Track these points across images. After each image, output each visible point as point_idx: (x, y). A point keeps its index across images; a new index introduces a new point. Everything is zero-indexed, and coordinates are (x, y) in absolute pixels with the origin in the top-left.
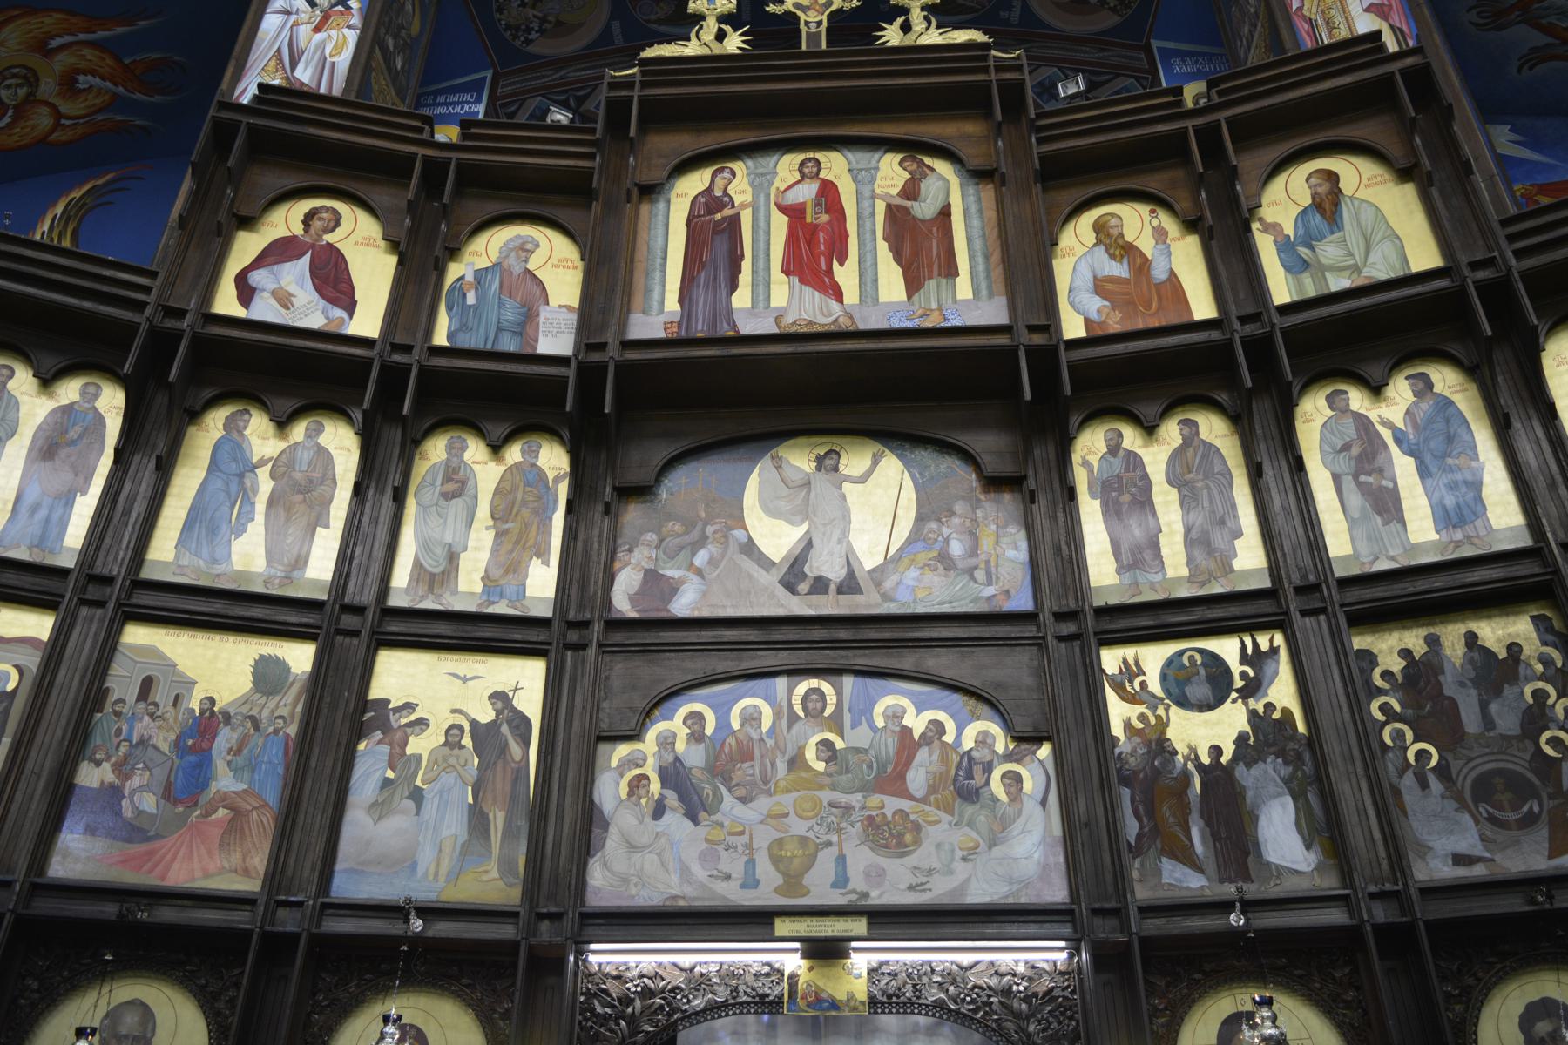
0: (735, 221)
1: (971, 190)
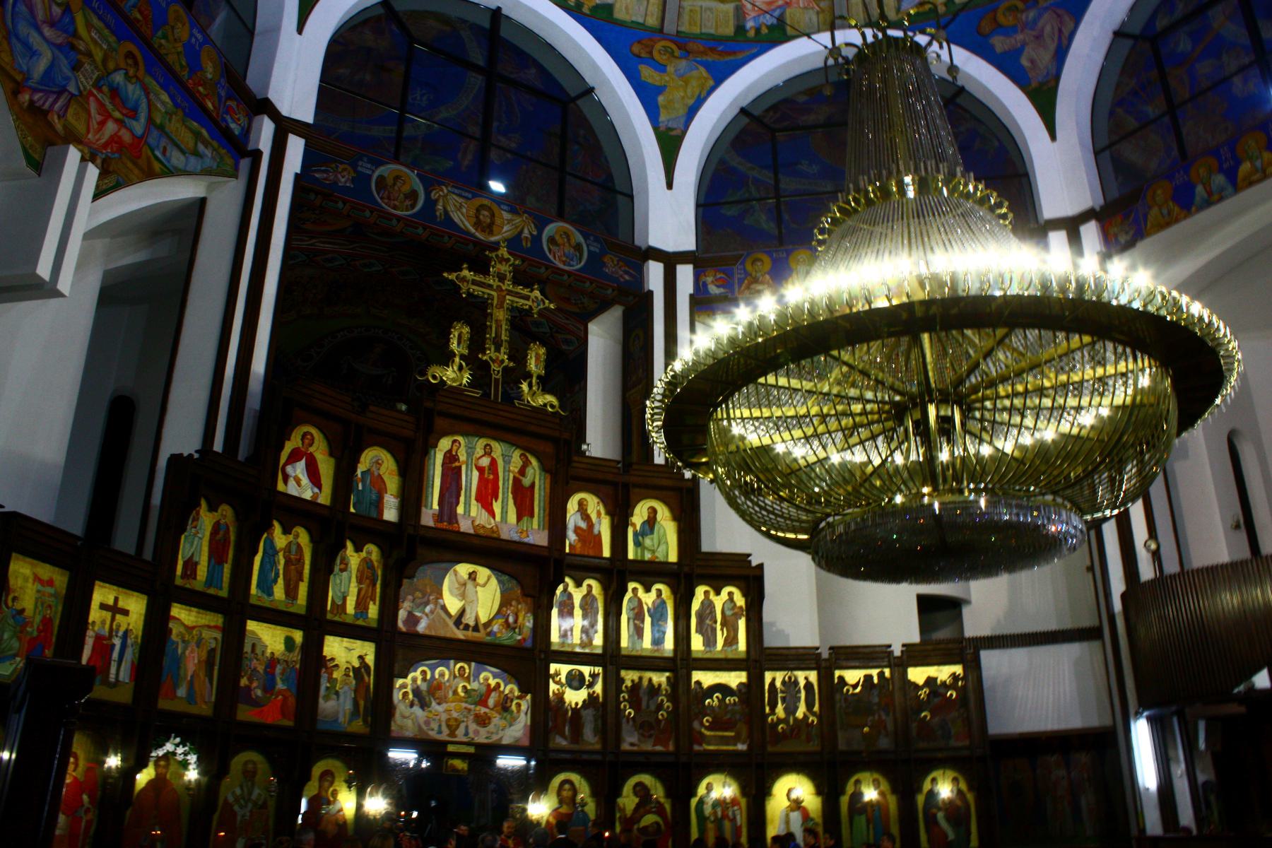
0: (460, 468)
1: (543, 473)
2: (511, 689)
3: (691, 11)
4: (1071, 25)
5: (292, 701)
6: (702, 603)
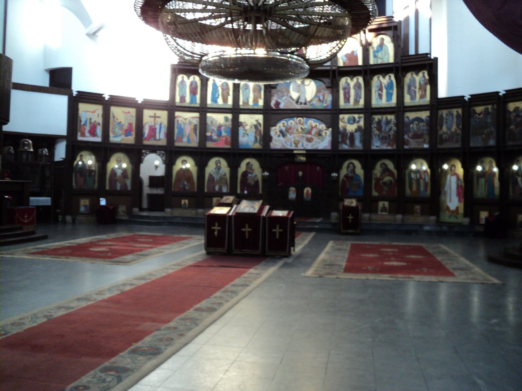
2: (322, 126)
5: (229, 139)
6: (410, 80)
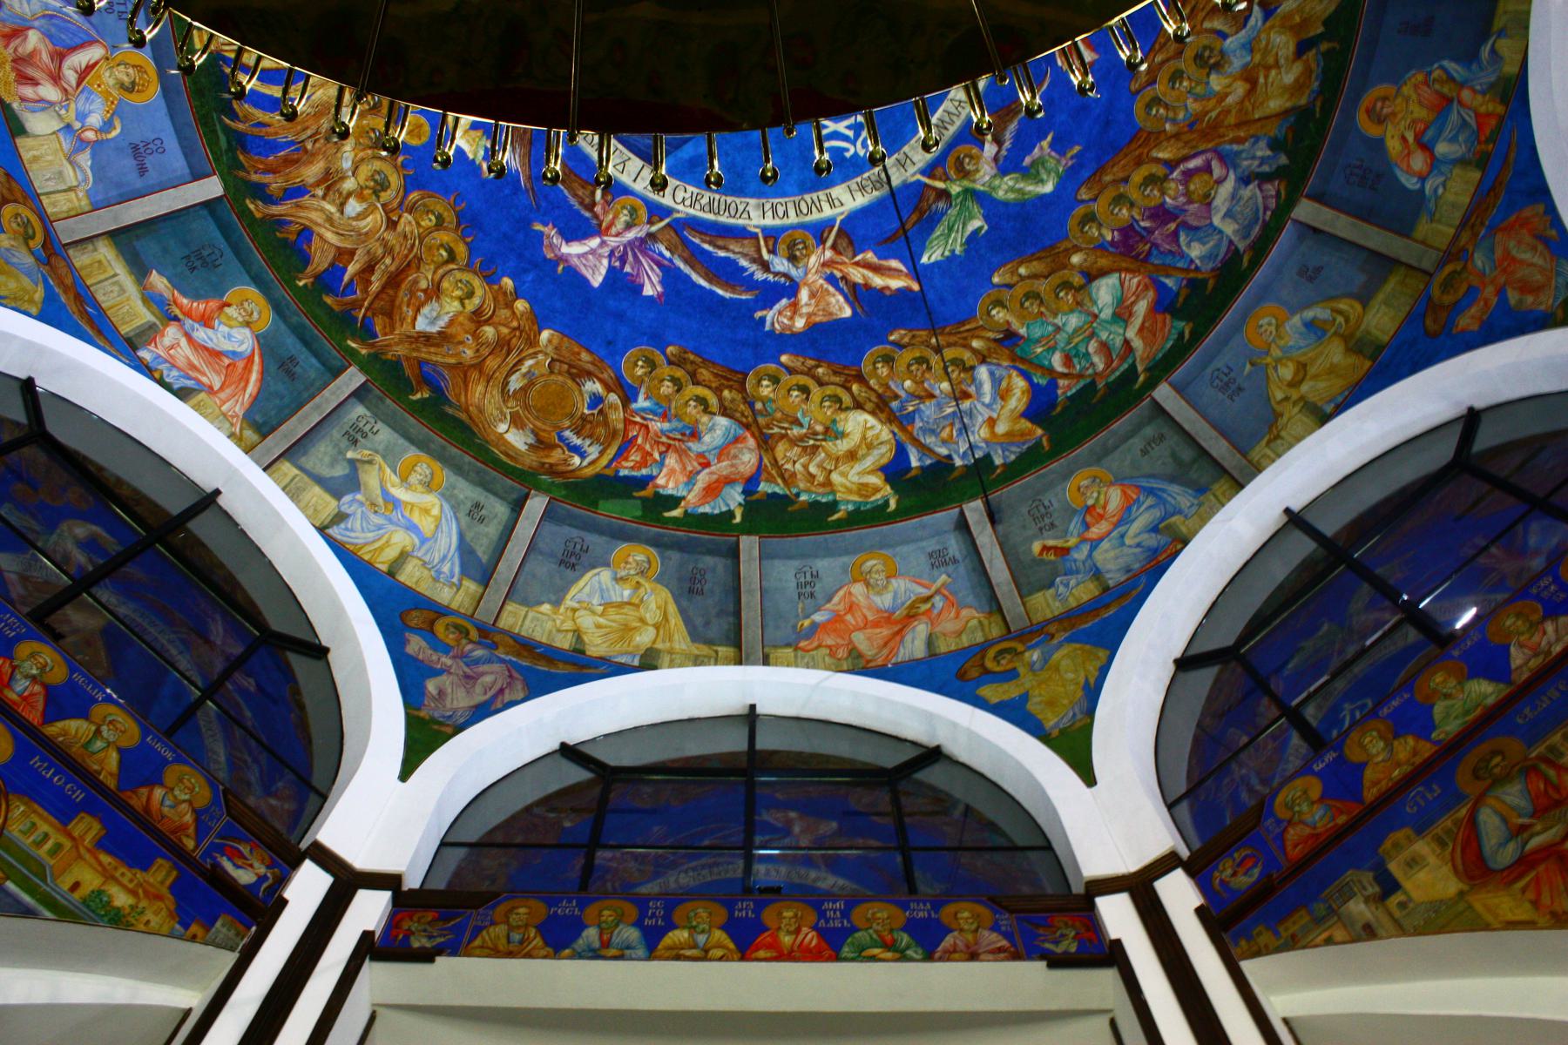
3: (100, 262)
4: (521, 695)
